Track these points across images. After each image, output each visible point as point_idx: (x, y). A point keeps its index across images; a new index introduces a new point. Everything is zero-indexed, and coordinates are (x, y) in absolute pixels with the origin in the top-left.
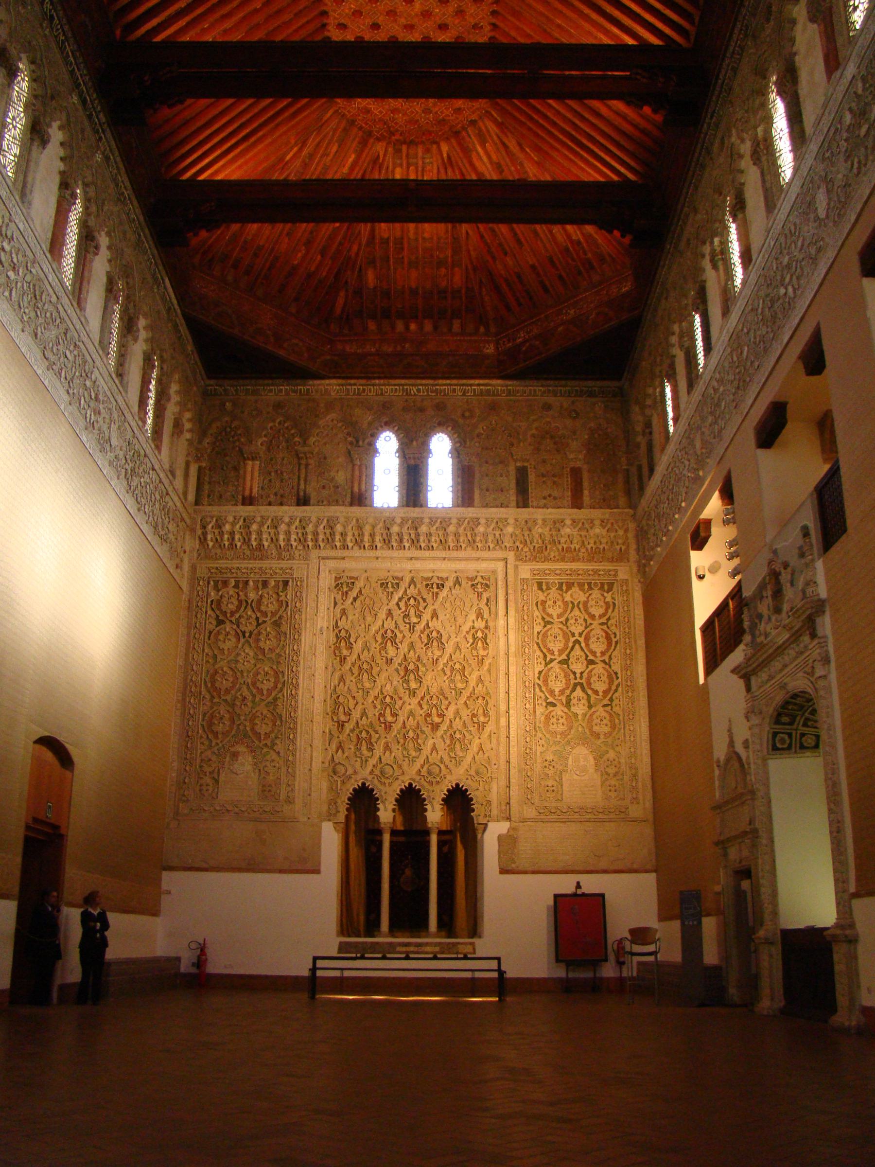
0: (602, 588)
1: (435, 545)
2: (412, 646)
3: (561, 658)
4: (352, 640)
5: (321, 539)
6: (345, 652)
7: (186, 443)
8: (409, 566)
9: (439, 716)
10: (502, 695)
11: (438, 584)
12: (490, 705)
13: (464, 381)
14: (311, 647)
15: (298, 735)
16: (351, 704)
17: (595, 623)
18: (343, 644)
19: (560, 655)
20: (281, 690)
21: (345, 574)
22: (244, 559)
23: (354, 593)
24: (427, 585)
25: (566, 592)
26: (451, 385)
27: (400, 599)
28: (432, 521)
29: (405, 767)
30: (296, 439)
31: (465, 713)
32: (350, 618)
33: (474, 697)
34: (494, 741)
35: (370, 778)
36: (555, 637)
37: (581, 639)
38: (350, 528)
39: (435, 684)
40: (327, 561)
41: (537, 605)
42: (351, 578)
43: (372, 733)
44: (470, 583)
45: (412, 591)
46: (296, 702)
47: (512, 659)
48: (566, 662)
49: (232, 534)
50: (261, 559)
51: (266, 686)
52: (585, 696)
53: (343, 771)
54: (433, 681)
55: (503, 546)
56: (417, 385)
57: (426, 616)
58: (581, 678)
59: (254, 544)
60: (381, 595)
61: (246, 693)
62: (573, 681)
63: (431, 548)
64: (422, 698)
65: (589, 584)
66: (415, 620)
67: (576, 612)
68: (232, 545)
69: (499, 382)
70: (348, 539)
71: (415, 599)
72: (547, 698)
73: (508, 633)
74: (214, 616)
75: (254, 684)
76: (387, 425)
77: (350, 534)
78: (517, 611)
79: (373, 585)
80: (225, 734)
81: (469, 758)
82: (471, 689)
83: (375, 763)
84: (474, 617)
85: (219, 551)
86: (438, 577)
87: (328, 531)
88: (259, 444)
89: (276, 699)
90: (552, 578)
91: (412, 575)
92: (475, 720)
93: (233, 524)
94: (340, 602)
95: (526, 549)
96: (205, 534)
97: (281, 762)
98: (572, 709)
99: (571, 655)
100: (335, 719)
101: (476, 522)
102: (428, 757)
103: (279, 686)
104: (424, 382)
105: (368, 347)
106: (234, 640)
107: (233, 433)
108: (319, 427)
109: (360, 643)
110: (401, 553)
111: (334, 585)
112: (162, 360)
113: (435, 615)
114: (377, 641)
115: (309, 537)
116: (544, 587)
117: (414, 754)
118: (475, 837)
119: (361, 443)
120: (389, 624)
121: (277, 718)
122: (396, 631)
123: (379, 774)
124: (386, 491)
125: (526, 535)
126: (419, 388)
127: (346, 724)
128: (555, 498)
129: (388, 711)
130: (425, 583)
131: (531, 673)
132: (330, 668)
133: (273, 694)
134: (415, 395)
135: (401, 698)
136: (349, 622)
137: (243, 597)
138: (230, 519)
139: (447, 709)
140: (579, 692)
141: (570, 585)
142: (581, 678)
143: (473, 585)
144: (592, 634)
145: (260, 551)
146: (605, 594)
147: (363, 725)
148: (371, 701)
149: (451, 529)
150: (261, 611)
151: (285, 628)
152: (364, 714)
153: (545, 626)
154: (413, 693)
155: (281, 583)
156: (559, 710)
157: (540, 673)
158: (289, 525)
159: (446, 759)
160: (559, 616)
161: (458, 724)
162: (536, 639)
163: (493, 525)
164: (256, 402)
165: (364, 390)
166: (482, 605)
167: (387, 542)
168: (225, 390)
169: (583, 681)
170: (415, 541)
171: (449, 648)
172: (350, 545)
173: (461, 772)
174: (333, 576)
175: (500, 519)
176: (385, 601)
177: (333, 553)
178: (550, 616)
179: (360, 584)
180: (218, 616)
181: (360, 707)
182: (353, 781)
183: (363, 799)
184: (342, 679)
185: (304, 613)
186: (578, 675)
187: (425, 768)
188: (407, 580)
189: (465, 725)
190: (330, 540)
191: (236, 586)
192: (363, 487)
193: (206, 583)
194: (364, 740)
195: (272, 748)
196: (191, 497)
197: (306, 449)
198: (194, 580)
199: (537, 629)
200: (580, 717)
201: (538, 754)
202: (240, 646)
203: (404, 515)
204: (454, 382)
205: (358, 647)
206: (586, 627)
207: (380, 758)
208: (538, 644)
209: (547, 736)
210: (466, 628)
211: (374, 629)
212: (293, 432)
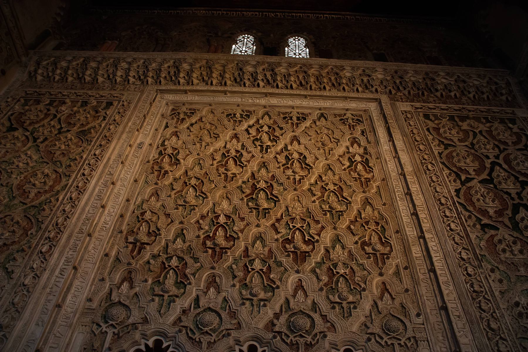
0: (502, 121)
1: (294, 86)
2: (264, 165)
3: (481, 178)
6: (167, 167)
8: (263, 101)
9: (306, 242)
10: (406, 218)
14: (120, 156)
17: (511, 150)
18: (166, 159)
19: (478, 175)
20: (58, 192)
22: (72, 88)
24: (284, 118)
26: (305, 13)
29: (244, 312)
31: (349, 241)
32: (183, 137)
35: (171, 331)
38: (198, 66)
39: (297, 204)
41: (428, 130)
42: (190, 109)
43: (190, 261)
44: (338, 118)
55: (374, 89)
56: (275, 12)
58: (521, 198)
59: (88, 79)
60: (226, 122)
62: (510, 203)
64: (278, 220)
65: (486, 119)
68: (64, 79)
70: (195, 75)
71: (269, 127)
75: (20, 187)
76: (248, 31)
82: (355, 212)
83: (186, 305)
84: (348, 144)
86: (298, 113)
90: (437, 112)
92: (369, 249)
95: (399, 94)
96: (36, 71)
100: (131, 239)
102: (287, 301)
106: (19, 145)
109: (190, 160)
110: (255, 90)
114: (214, 159)
115: (150, 74)
117: (262, 295)
125: (398, 82)
127: (148, 247)
129: (220, 232)
130: (282, 116)
132: (141, 182)
135: (243, 219)
136: (180, 142)
137: (53, 111)
139: (319, 235)
141: (463, 119)
142: (521, 198)
144: (512, 157)
145: (93, 83)
146: (511, 125)
147: (175, 250)
148: (193, 221)
149: (311, 72)
150: (70, 124)
152: (181, 234)
153: (446, 148)
155: (104, 105)
157: (458, 191)
159: (324, 306)
162: (438, 158)
163: (360, 72)
165: (227, 14)
166: (357, 133)
167: (239, 81)
170: (271, 81)
172: (195, 81)
173: (355, 328)
174: (171, 108)
175: (368, 68)
178: (451, 140)
180: (12, 124)
182: (137, 336)
184: (156, 194)
185: (121, 127)
187: (283, 319)
191: (50, 104)
193: (15, 101)
203: (260, 61)
206: (501, 152)
207: (197, 300)
208: (443, 163)
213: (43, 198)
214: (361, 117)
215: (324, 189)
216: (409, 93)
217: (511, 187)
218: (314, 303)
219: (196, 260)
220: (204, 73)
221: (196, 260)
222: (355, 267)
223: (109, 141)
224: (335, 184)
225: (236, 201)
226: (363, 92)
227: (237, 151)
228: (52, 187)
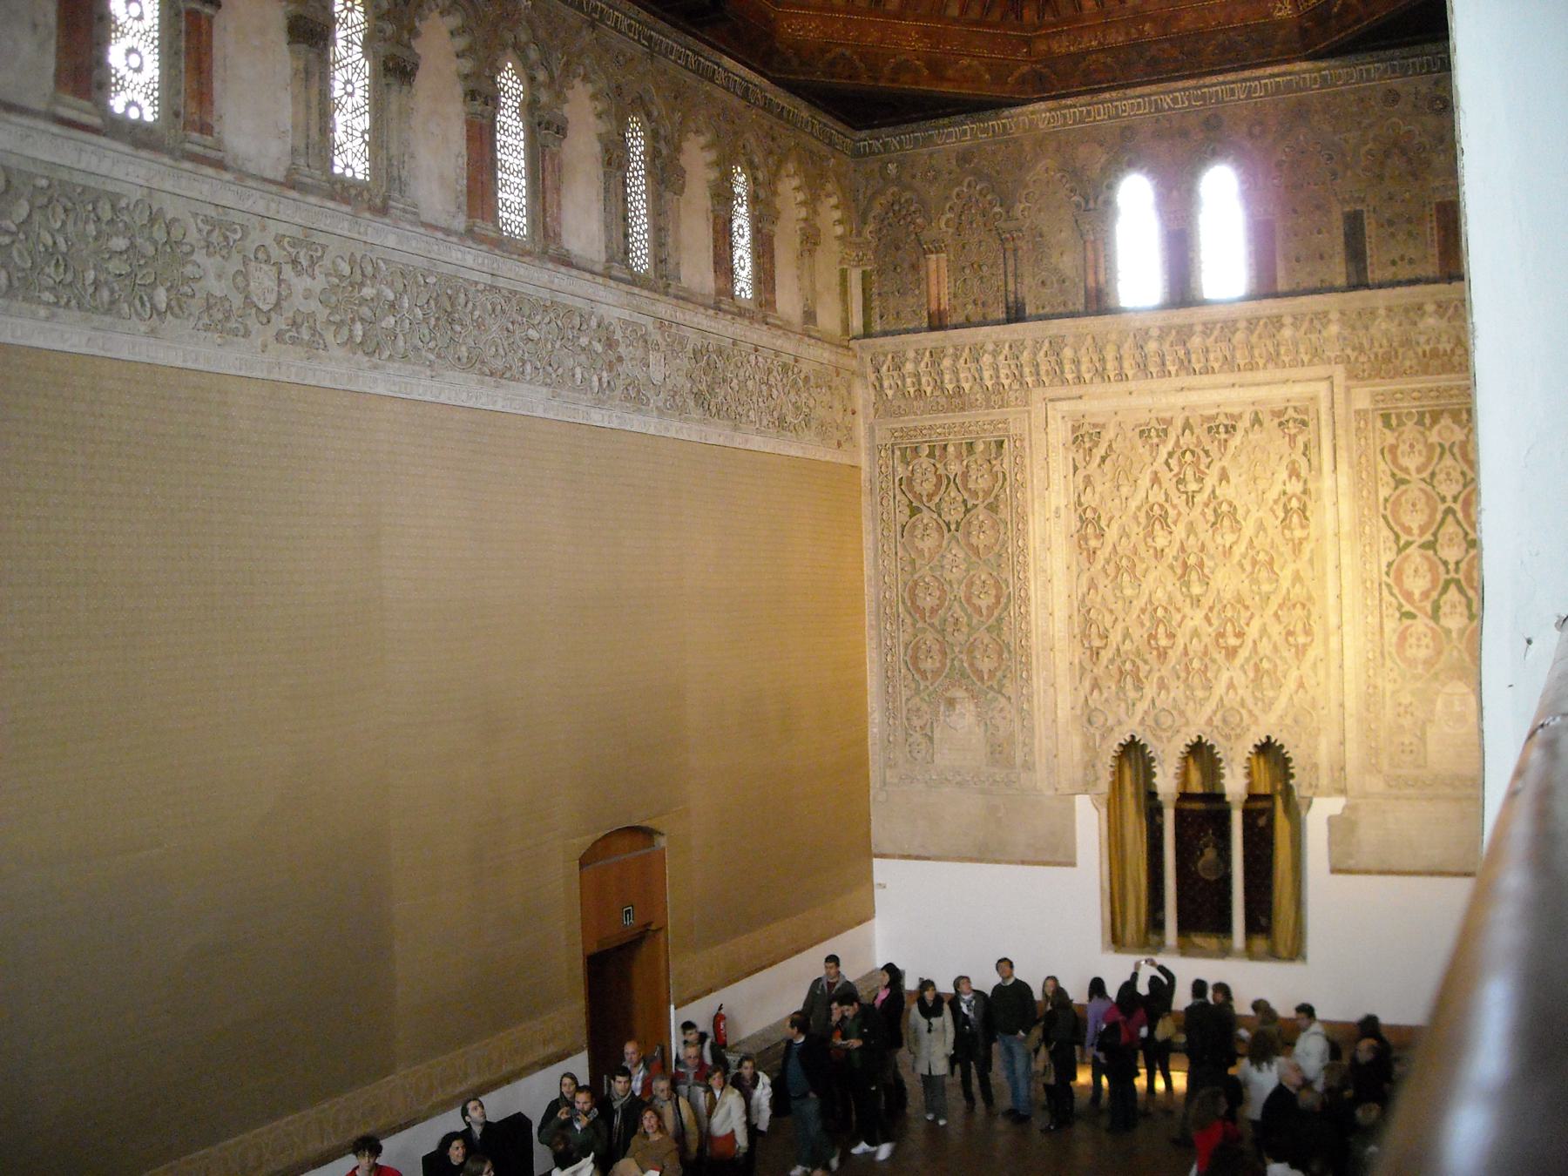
1: (1216, 366)
2: (1191, 529)
4: (1103, 523)
5: (1042, 372)
6: (1093, 543)
7: (836, 246)
8: (1180, 400)
11: (1226, 427)
12: (1314, 617)
13: (1247, 74)
14: (1043, 540)
15: (1034, 672)
16: (1108, 619)
18: (1090, 530)
21: (1087, 420)
23: (1100, 451)
24: (1210, 429)
25: (1430, 429)
27: (1170, 455)
28: (1208, 328)
29: (1189, 714)
30: (997, 209)
31: (1276, 630)
32: (1099, 489)
33: (1289, 604)
34: (1321, 673)
36: (1414, 505)
37: (1457, 507)
40: (1059, 405)
42: (1095, 426)
44: (1276, 421)
45: (1188, 440)
46: (1028, 623)
47: (1345, 544)
48: (1431, 545)
49: (917, 375)
50: (963, 409)
51: (984, 602)
52: (1463, 600)
53: (1102, 719)
54: (1226, 581)
57: (1211, 480)
58: (1457, 570)
59: (950, 387)
60: (1141, 450)
61: (959, 613)
62: (1443, 577)
63: (1208, 371)
64: (1211, 609)
66: (1193, 486)
67: (1448, 461)
69: (1305, 65)
70: (1084, 368)
71: (1193, 453)
72: (1400, 606)
73: (1337, 498)
74: (905, 501)
77: (1085, 360)
78: (1351, 466)
79: (1130, 434)
80: (936, 673)
81: (1283, 701)
84: (1283, 474)
85: (902, 403)
87: (1053, 359)
88: (943, 225)
89: (1000, 620)
91: (1187, 413)
93: (917, 362)
94: (1080, 464)
95: (1363, 359)
96: (880, 380)
97: (1014, 712)
98: (1443, 622)
99: (1439, 536)
101: (1277, 322)
103: (1004, 600)
104: (1180, 84)
105: (1086, 39)
106: (935, 535)
107: (904, 212)
108: (1026, 186)
110: (1166, 383)
111: (1071, 439)
112: (751, 167)
113: (1224, 476)
114: (1139, 524)
115: (1027, 370)
116: (1394, 422)
118: (1299, 814)
119: (1091, 205)
120: (1157, 496)
121: (1002, 648)
122: (1167, 506)
123: (1152, 723)
124: (1138, 277)
126: (1176, 96)
128: (1411, 261)
129: (1161, 629)
130: (1206, 426)
131: (1375, 567)
132: (1074, 567)
133: (996, 614)
134: (1170, 109)
135: (1178, 610)
136: (1097, 496)
137: (941, 471)
138: (911, 354)
140: (1453, 592)
141: (1436, 417)
142: (1457, 570)
143: (1280, 424)
151: (1004, 513)
152: (1126, 635)
154: (1196, 602)
156: (1421, 625)
157: (1389, 565)
158: (995, 354)
159: (1249, 701)
160: (1419, 470)
161: (1265, 647)
163: (1306, 325)
164: (931, 155)
165: (1089, 112)
167: (1143, 367)
168: (884, 144)
169: (1461, 576)
171: (1249, 528)
172: (1087, 377)
176: (1148, 459)
177: (1061, 391)
178: (1406, 470)
179: (1108, 435)
181: (1120, 626)
183: (1133, 754)
184: (1092, 585)
186: (1452, 567)
187: (1219, 715)
188: (1179, 423)
189: (1276, 649)
190: (1058, 374)
191: (931, 455)
192: (1102, 278)
194: (1130, 675)
195: (1000, 692)
196: (857, 323)
197: (1011, 225)
198: (875, 450)
199: (1384, 492)
200: (1454, 635)
201: (1388, 694)
202: (945, 543)
204: (1231, 77)
205: (1112, 534)
206: (1465, 486)
208: (1384, 517)
209: (1403, 666)
210: (1272, 494)
211: (1133, 504)
212: (989, 197)
213: (996, 614)
214: (1306, 411)
215: (1254, 563)
216: (1376, 355)
217: (1451, 554)
218: (1242, 700)
219: (1146, 662)
220: (1095, 358)
221: (1146, 662)
222: (1278, 662)
223: (1026, 523)
224: (1267, 553)
225: (1170, 588)
226: (1311, 363)
227: (1161, 506)
228: (998, 598)
